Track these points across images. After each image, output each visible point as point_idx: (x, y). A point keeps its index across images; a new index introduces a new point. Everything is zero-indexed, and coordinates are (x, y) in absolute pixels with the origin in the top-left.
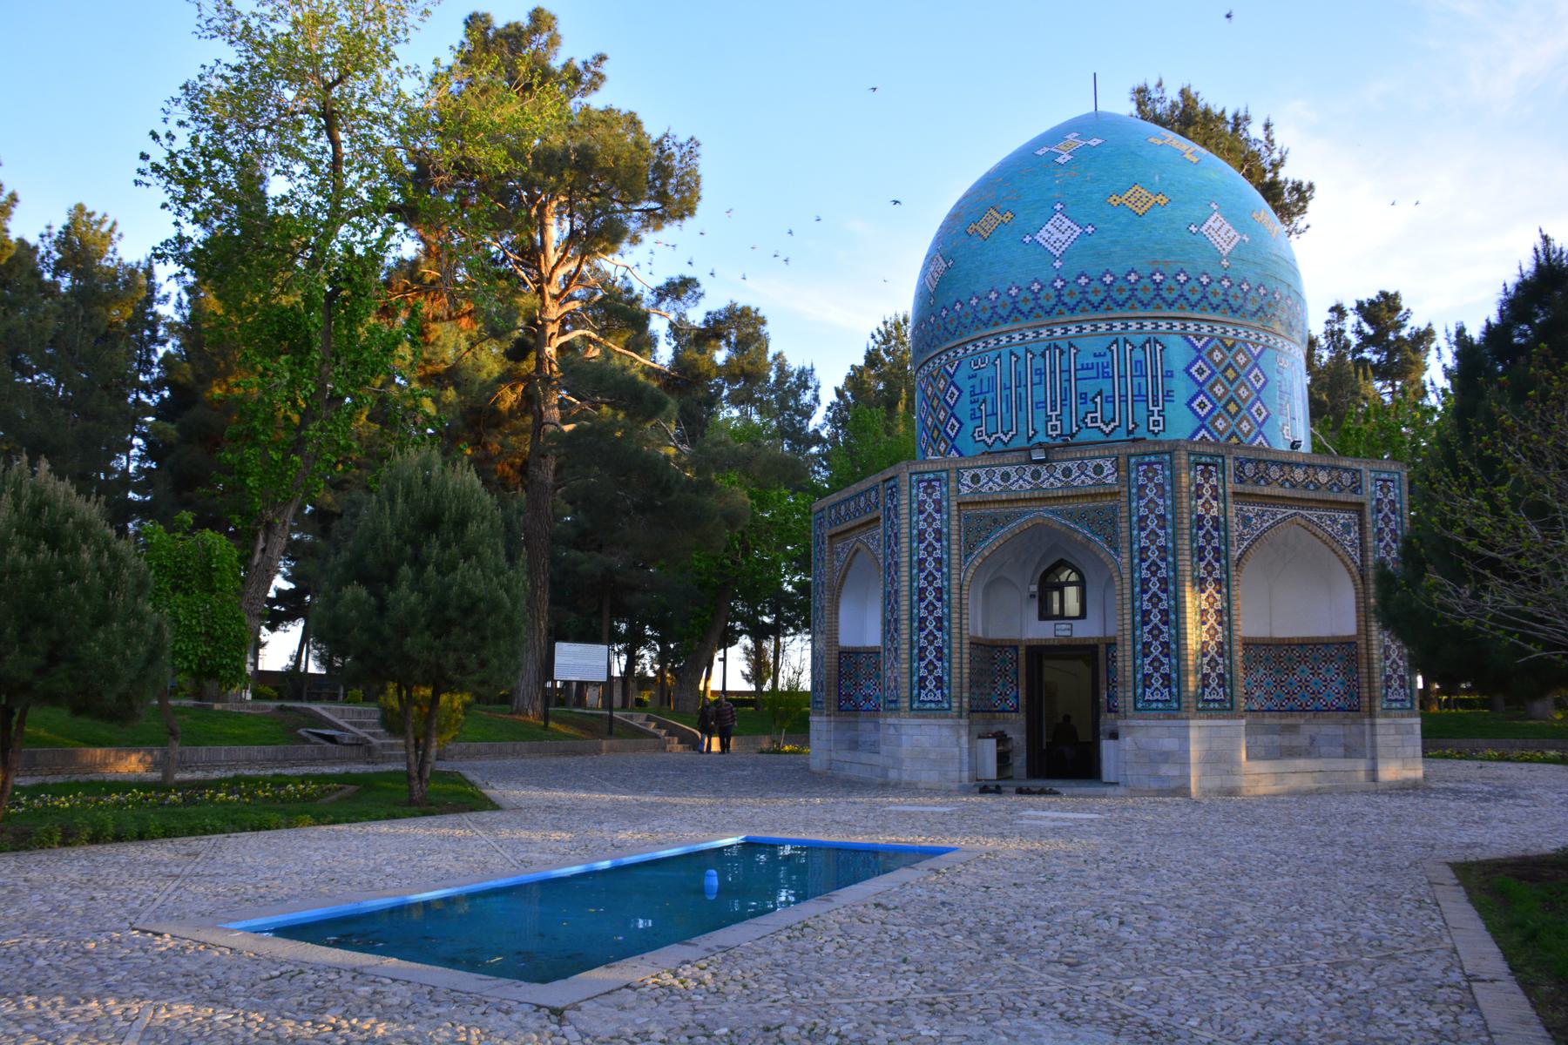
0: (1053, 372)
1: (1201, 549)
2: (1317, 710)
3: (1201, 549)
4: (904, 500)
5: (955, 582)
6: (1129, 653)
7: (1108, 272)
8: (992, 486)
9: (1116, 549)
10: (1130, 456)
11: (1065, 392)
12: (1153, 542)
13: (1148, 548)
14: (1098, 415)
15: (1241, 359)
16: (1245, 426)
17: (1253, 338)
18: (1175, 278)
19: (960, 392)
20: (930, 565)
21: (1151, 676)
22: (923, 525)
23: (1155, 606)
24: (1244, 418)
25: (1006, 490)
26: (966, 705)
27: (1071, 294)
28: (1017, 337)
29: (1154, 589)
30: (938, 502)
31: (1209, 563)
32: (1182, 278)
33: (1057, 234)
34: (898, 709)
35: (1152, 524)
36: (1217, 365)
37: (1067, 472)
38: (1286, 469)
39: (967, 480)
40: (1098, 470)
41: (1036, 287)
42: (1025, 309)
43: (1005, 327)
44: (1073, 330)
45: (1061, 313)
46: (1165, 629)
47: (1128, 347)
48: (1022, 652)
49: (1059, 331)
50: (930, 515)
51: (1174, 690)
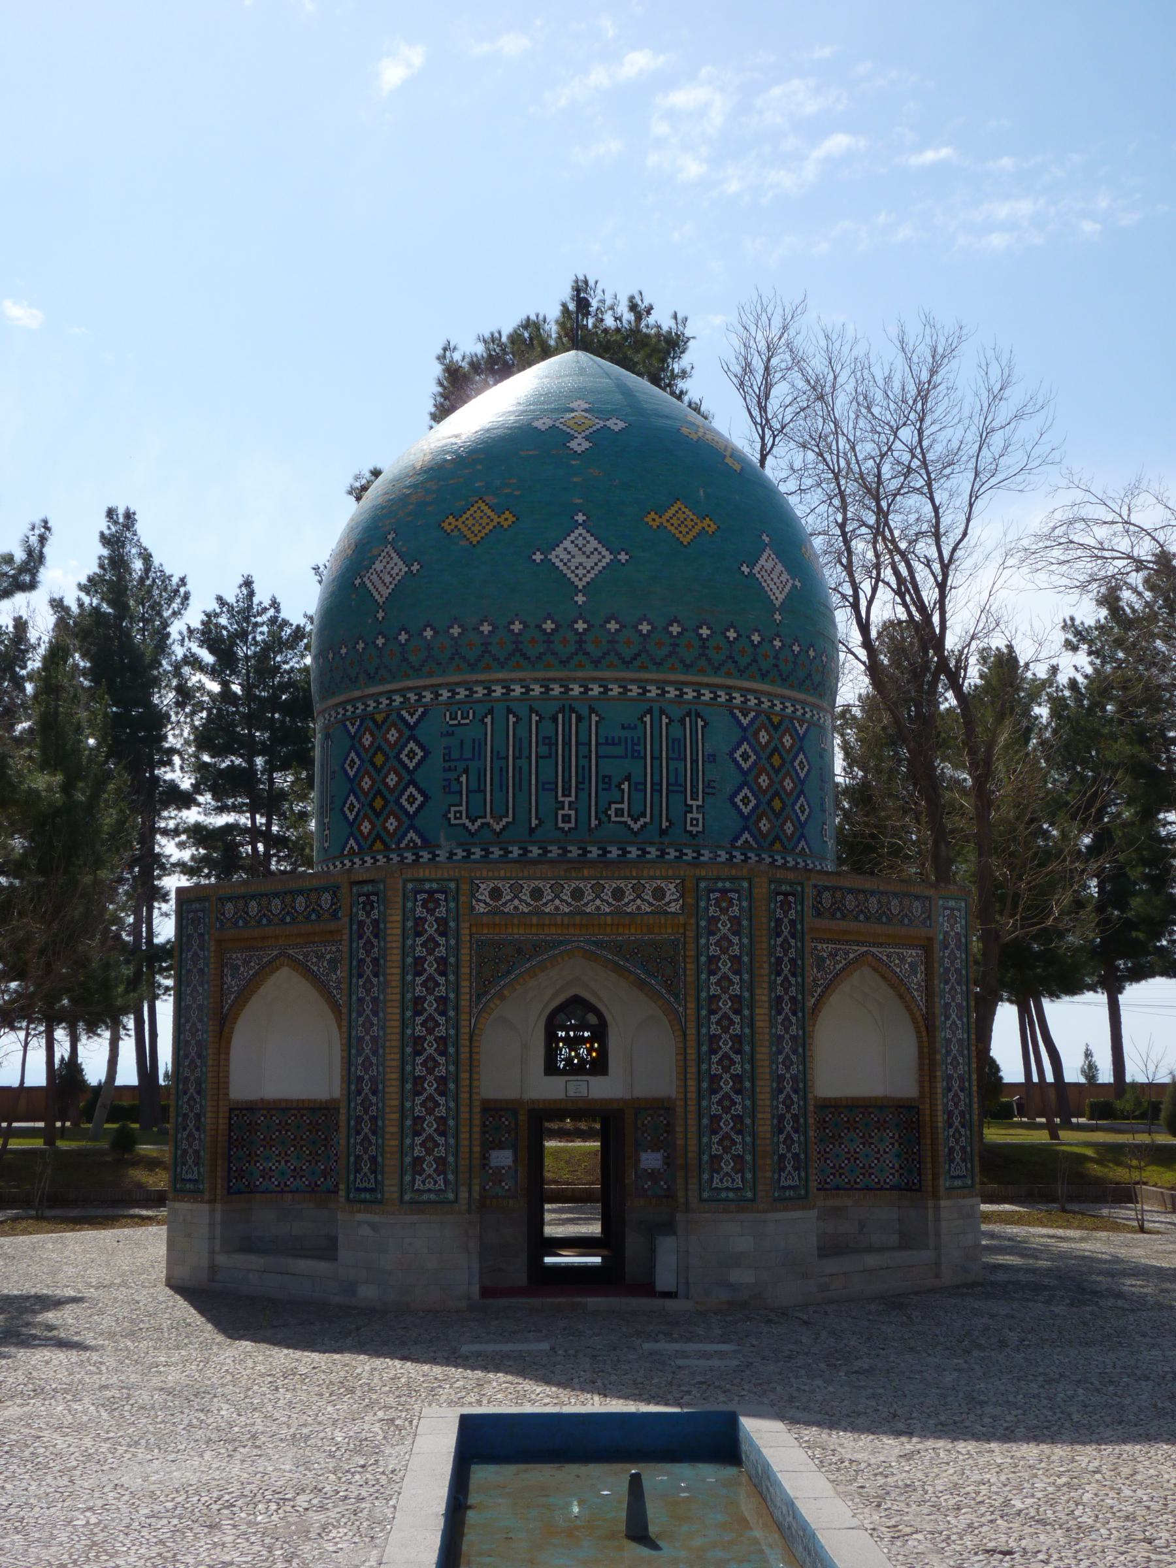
0: (567, 743)
1: (779, 999)
2: (868, 1188)
3: (779, 999)
4: (395, 916)
5: (465, 1030)
6: (693, 1129)
7: (644, 618)
9: (676, 996)
10: (699, 879)
12: (725, 990)
13: (718, 998)
14: (625, 806)
15: (787, 741)
16: (789, 828)
17: (799, 713)
18: (724, 633)
20: (430, 1006)
21: (719, 1158)
22: (420, 951)
23: (726, 1070)
24: (788, 818)
25: (538, 912)
26: (476, 1195)
28: (518, 690)
29: (726, 1049)
30: (442, 922)
31: (787, 1018)
32: (732, 634)
34: (381, 1202)
35: (725, 967)
37: (618, 894)
38: (861, 897)
39: (484, 894)
40: (659, 893)
41: (549, 626)
43: (500, 676)
44: (596, 690)
45: (580, 666)
46: (738, 1099)
47: (665, 720)
48: (523, 1117)
49: (576, 690)
50: (431, 939)
51: (749, 1176)
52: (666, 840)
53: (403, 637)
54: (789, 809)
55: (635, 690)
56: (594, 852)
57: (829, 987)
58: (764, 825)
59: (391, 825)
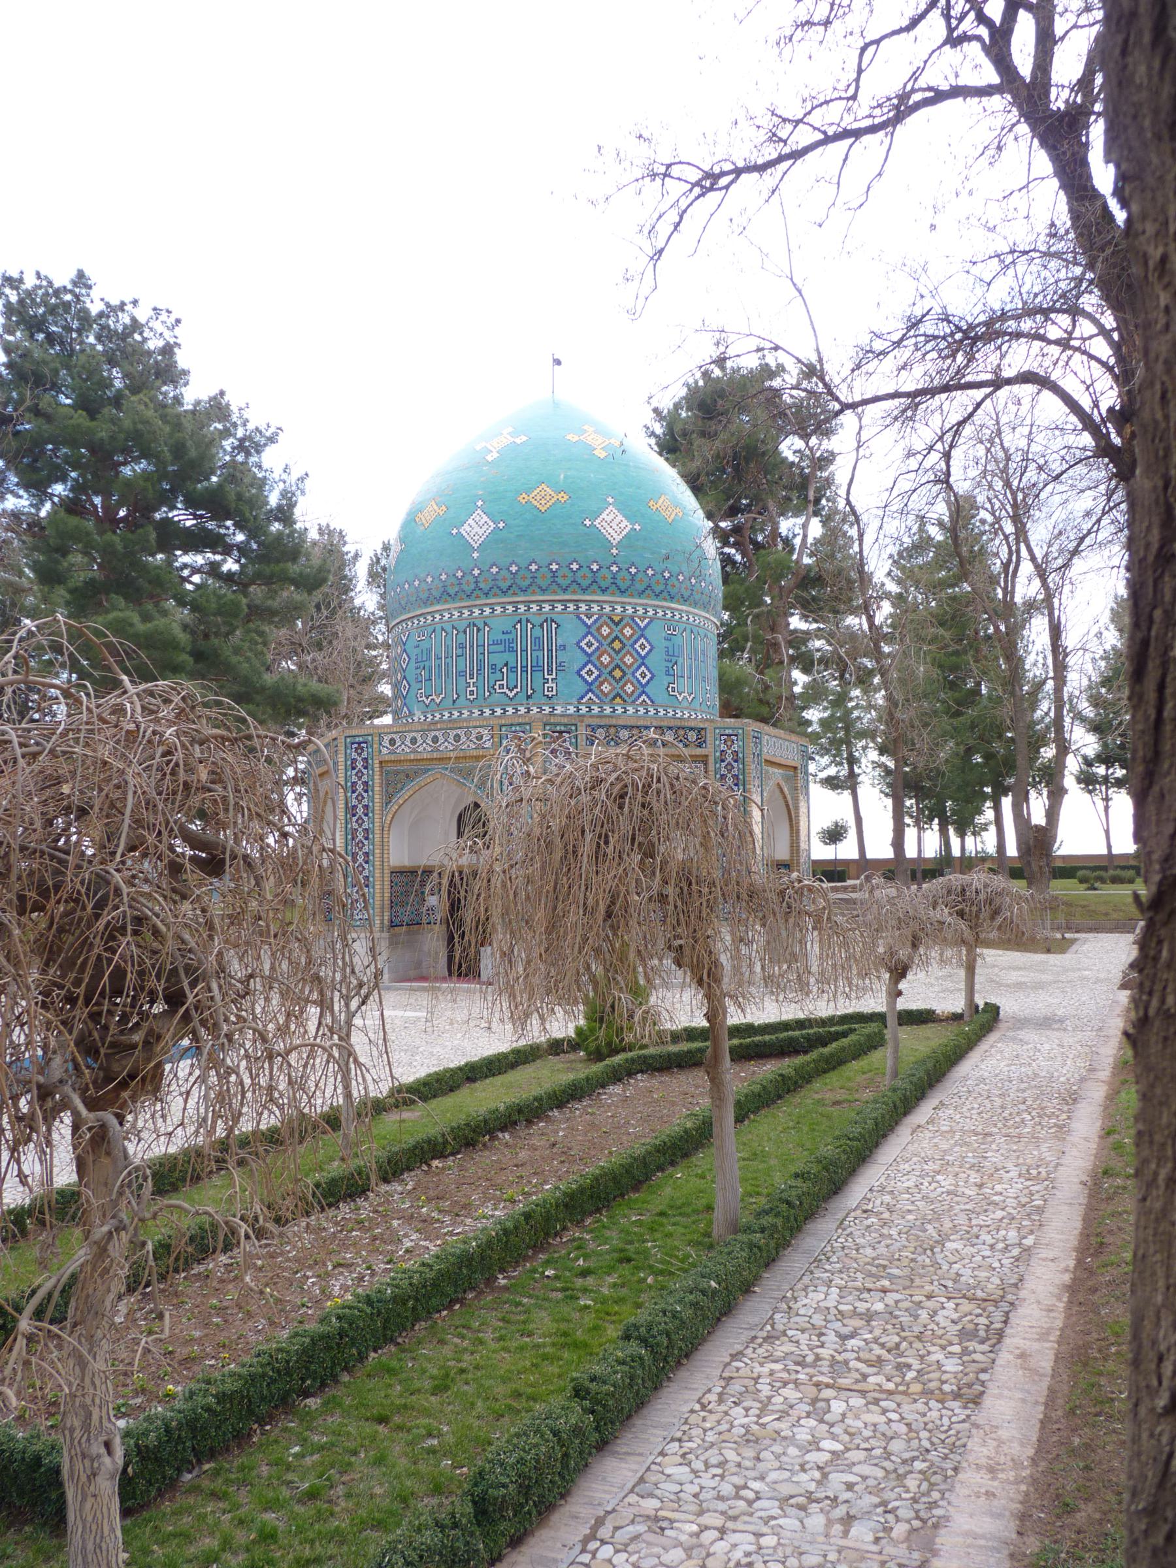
0: (472, 646)
7: (514, 562)
8: (404, 749)
11: (481, 663)
16: (629, 688)
22: (355, 779)
24: (628, 681)
25: (415, 751)
27: (486, 580)
28: (447, 615)
32: (575, 566)
33: (477, 528)
36: (605, 638)
37: (457, 738)
39: (386, 743)
40: (479, 738)
41: (459, 574)
42: (452, 591)
44: (488, 611)
45: (478, 597)
49: (477, 612)
52: (531, 701)
54: (629, 676)
55: (510, 608)
56: (488, 712)
58: (606, 688)
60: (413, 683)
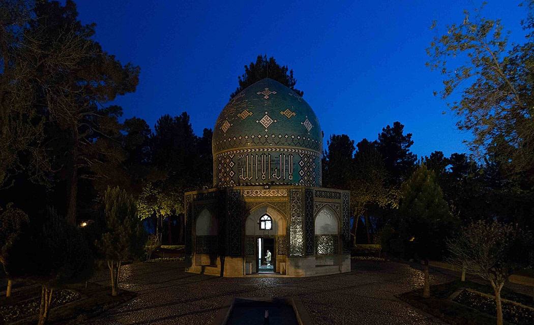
0: (264, 161)
9: (286, 213)
15: (311, 160)
19: (235, 164)
36: (306, 162)
41: (260, 136)
53: (230, 139)
57: (319, 211)
59: (228, 179)
60: (237, 172)
